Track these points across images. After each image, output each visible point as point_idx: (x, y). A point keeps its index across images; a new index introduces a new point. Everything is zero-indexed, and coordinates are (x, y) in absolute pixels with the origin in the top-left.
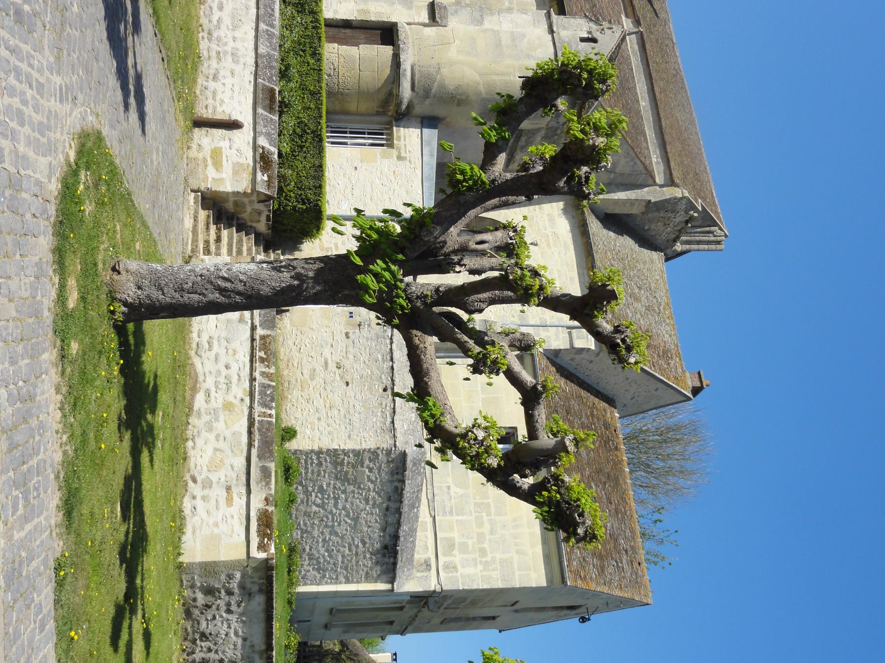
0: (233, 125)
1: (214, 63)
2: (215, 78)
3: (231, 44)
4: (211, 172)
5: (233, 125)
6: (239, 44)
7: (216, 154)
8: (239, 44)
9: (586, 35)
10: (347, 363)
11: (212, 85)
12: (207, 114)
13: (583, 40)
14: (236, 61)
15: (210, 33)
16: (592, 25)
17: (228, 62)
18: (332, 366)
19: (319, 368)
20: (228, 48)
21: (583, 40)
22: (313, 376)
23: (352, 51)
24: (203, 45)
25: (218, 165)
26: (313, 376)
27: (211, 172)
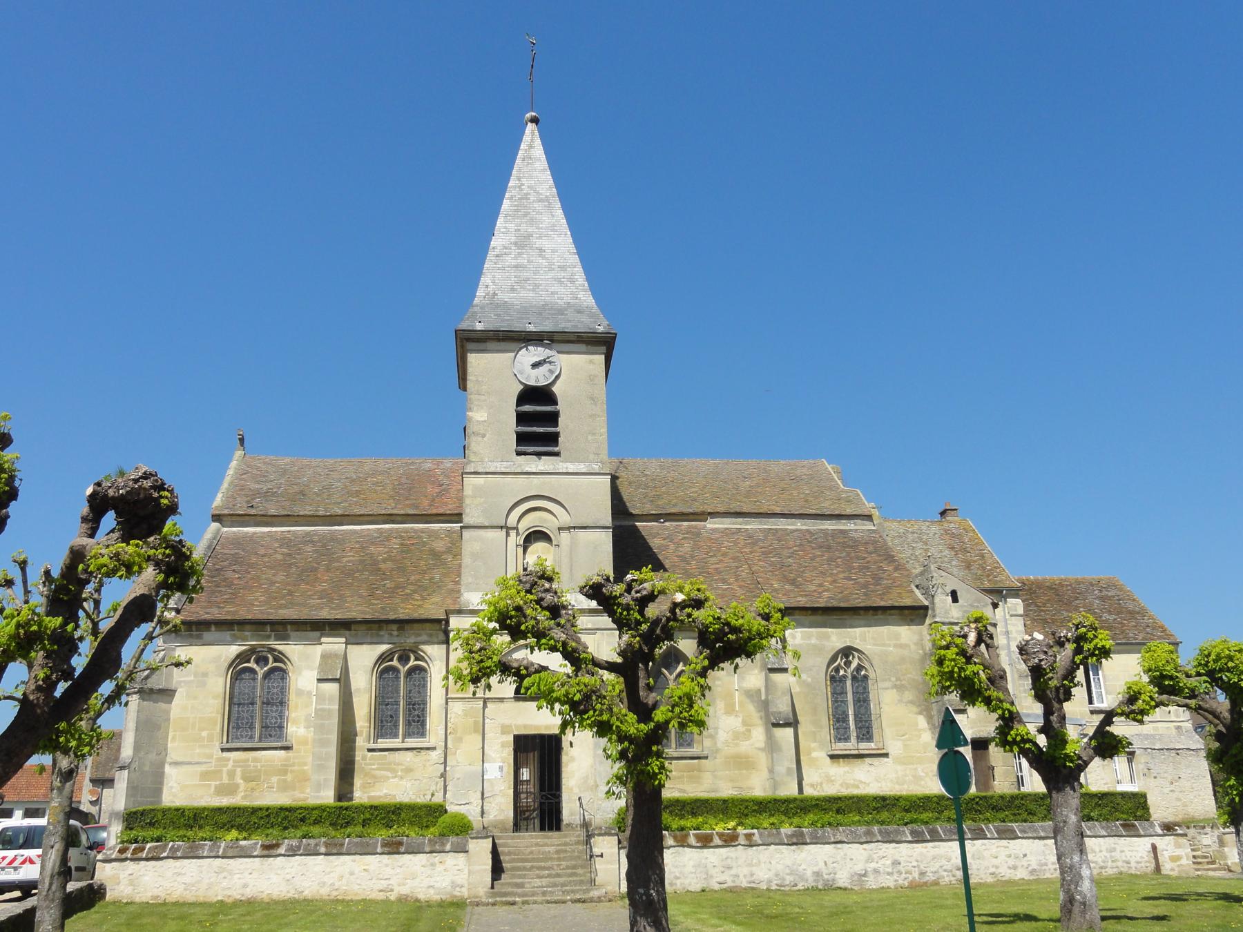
0: (1154, 848)
1: (1120, 864)
2: (1128, 863)
3: (1104, 853)
4: (1184, 861)
5: (1154, 848)
6: (1104, 848)
7: (1174, 859)
8: (1104, 848)
9: (950, 598)
10: (1170, 778)
11: (1133, 865)
12: (1153, 865)
13: (955, 600)
14: (1114, 850)
15: (1101, 868)
16: (940, 590)
17: (1117, 855)
18: (1172, 787)
19: (1175, 795)
20: (1108, 855)
21: (955, 600)
22: (1180, 800)
23: (998, 772)
24: (1110, 871)
25: (1178, 858)
26: (1180, 800)
27: (1184, 861)
